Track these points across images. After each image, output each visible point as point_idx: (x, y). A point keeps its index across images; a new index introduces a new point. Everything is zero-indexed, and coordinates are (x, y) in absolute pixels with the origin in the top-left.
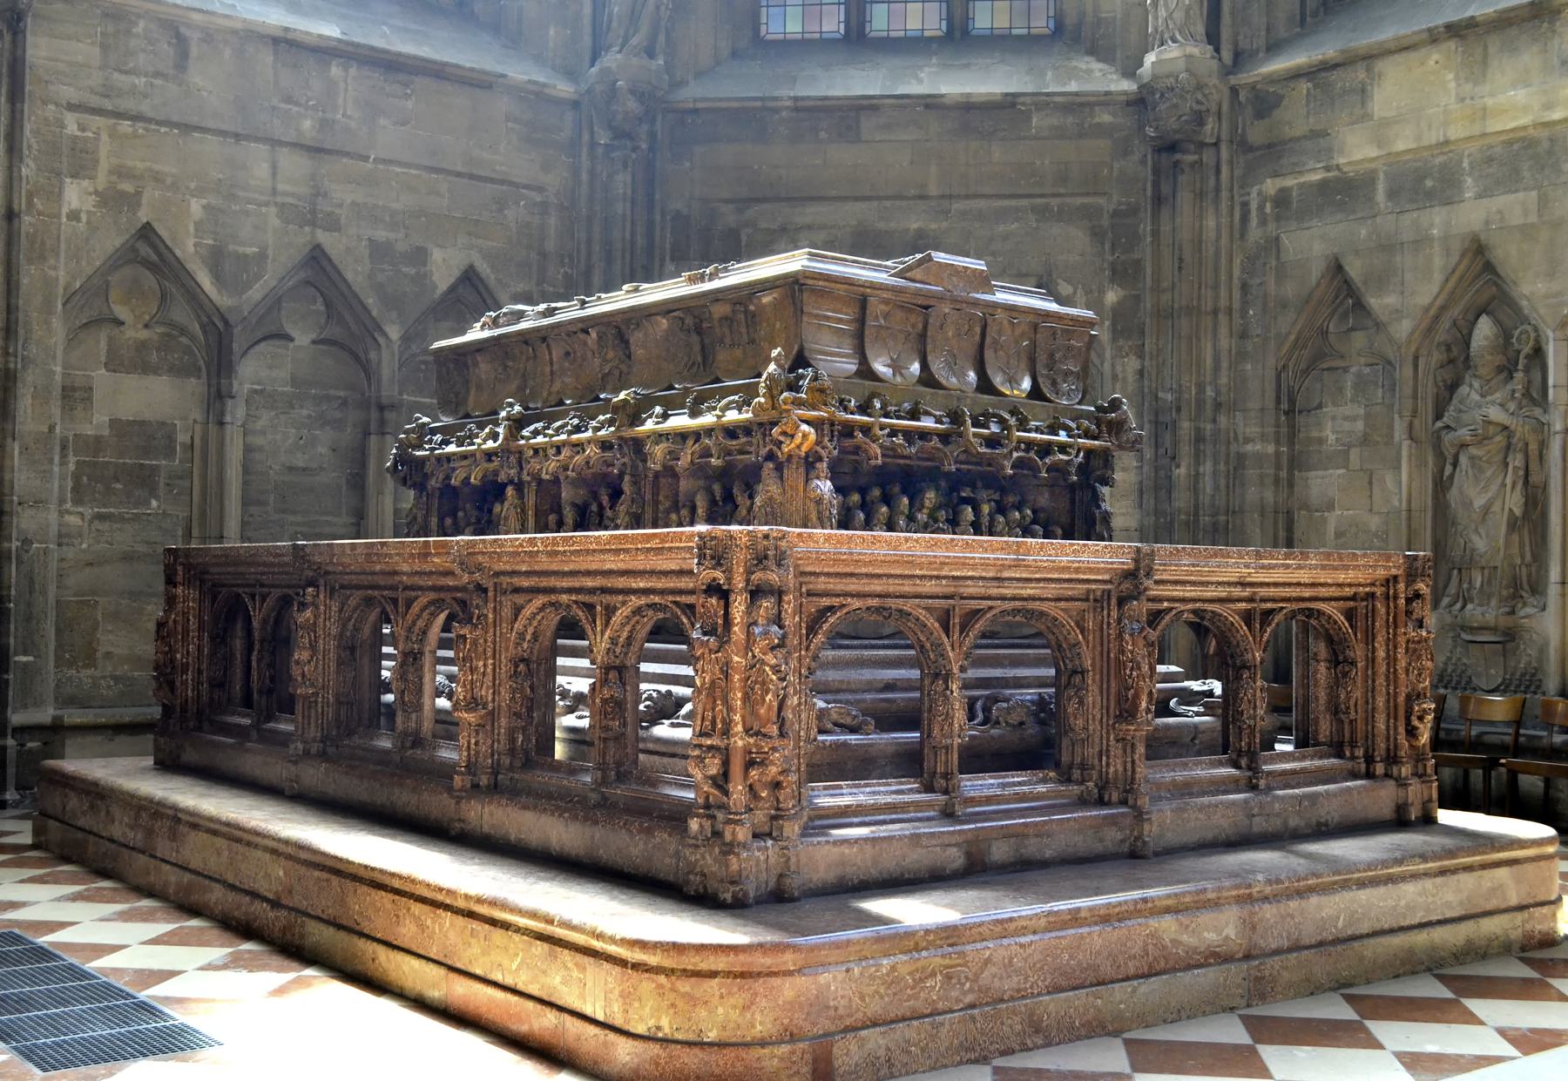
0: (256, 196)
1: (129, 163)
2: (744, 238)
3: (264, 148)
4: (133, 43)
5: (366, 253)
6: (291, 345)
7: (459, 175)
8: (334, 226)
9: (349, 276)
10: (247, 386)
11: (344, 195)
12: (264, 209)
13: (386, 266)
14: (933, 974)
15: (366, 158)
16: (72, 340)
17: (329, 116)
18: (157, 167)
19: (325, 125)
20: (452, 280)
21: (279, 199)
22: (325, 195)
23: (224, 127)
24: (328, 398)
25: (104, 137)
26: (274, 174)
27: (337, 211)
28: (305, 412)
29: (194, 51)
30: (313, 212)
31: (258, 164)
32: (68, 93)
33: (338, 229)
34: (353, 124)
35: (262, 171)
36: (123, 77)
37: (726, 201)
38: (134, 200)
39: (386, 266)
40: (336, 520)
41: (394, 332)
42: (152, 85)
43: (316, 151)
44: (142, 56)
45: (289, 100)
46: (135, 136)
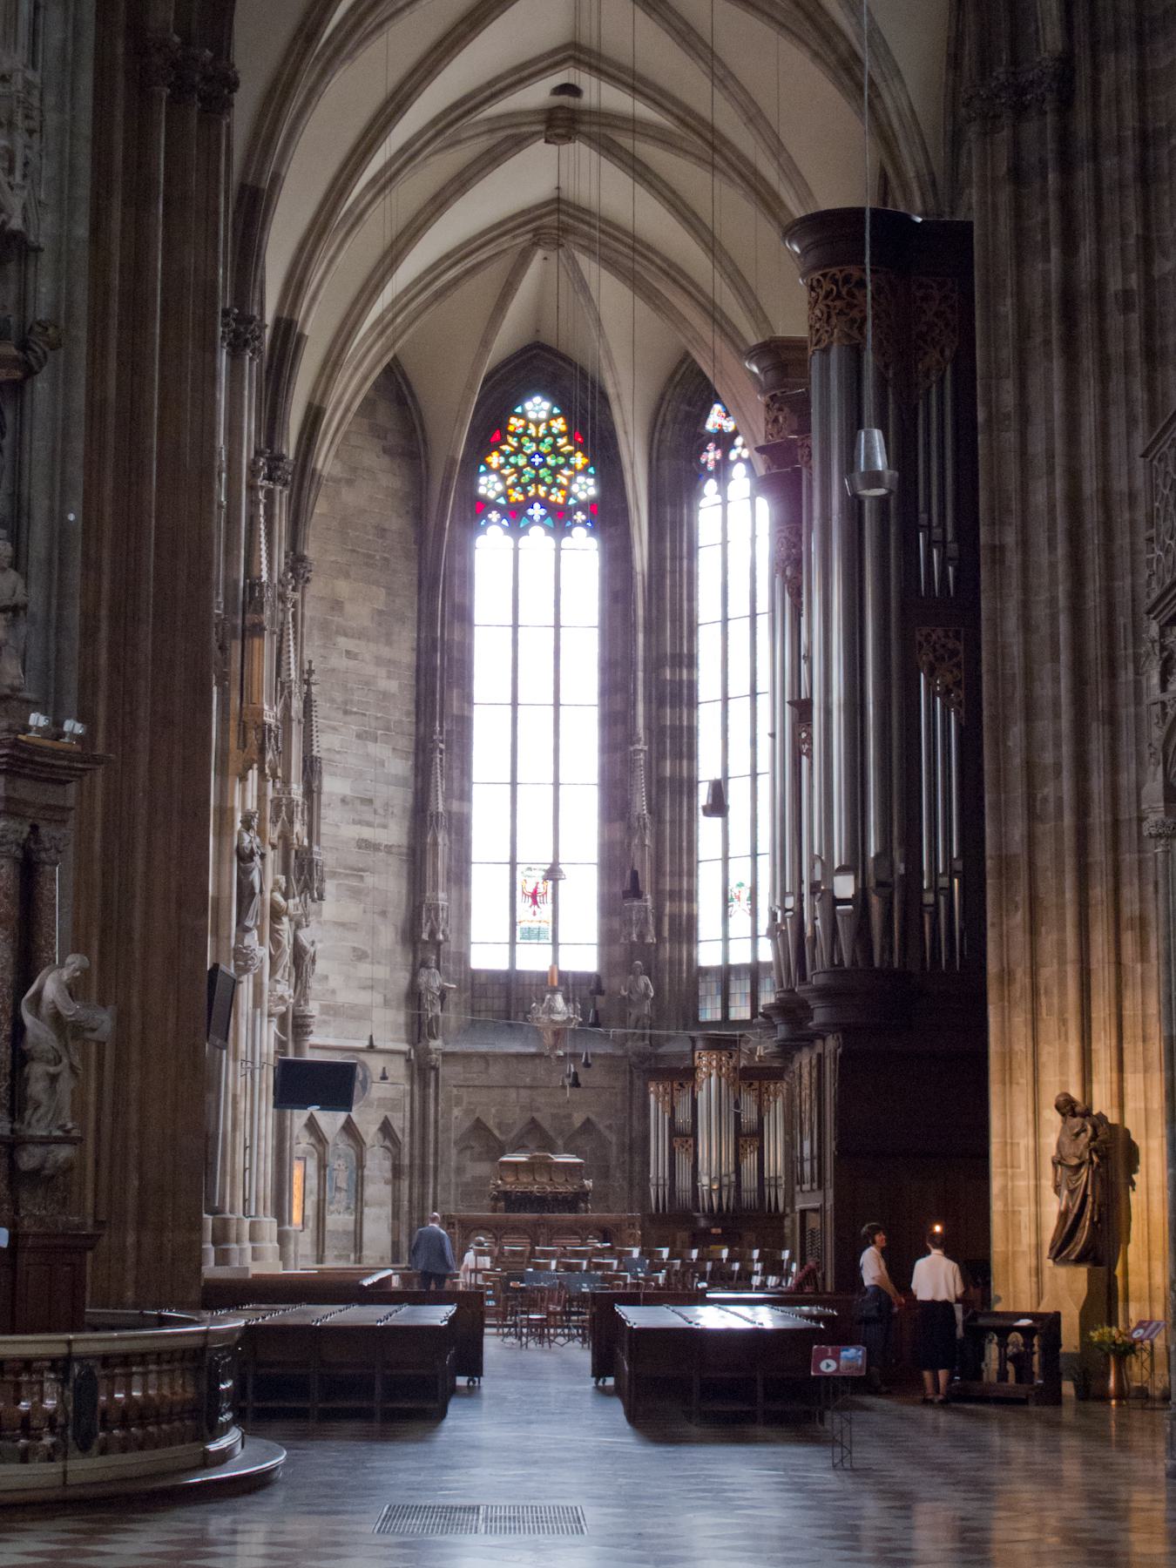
8: (538, 1110)
16: (461, 1152)
19: (534, 1079)
31: (513, 1094)
38: (473, 1111)
43: (531, 1087)
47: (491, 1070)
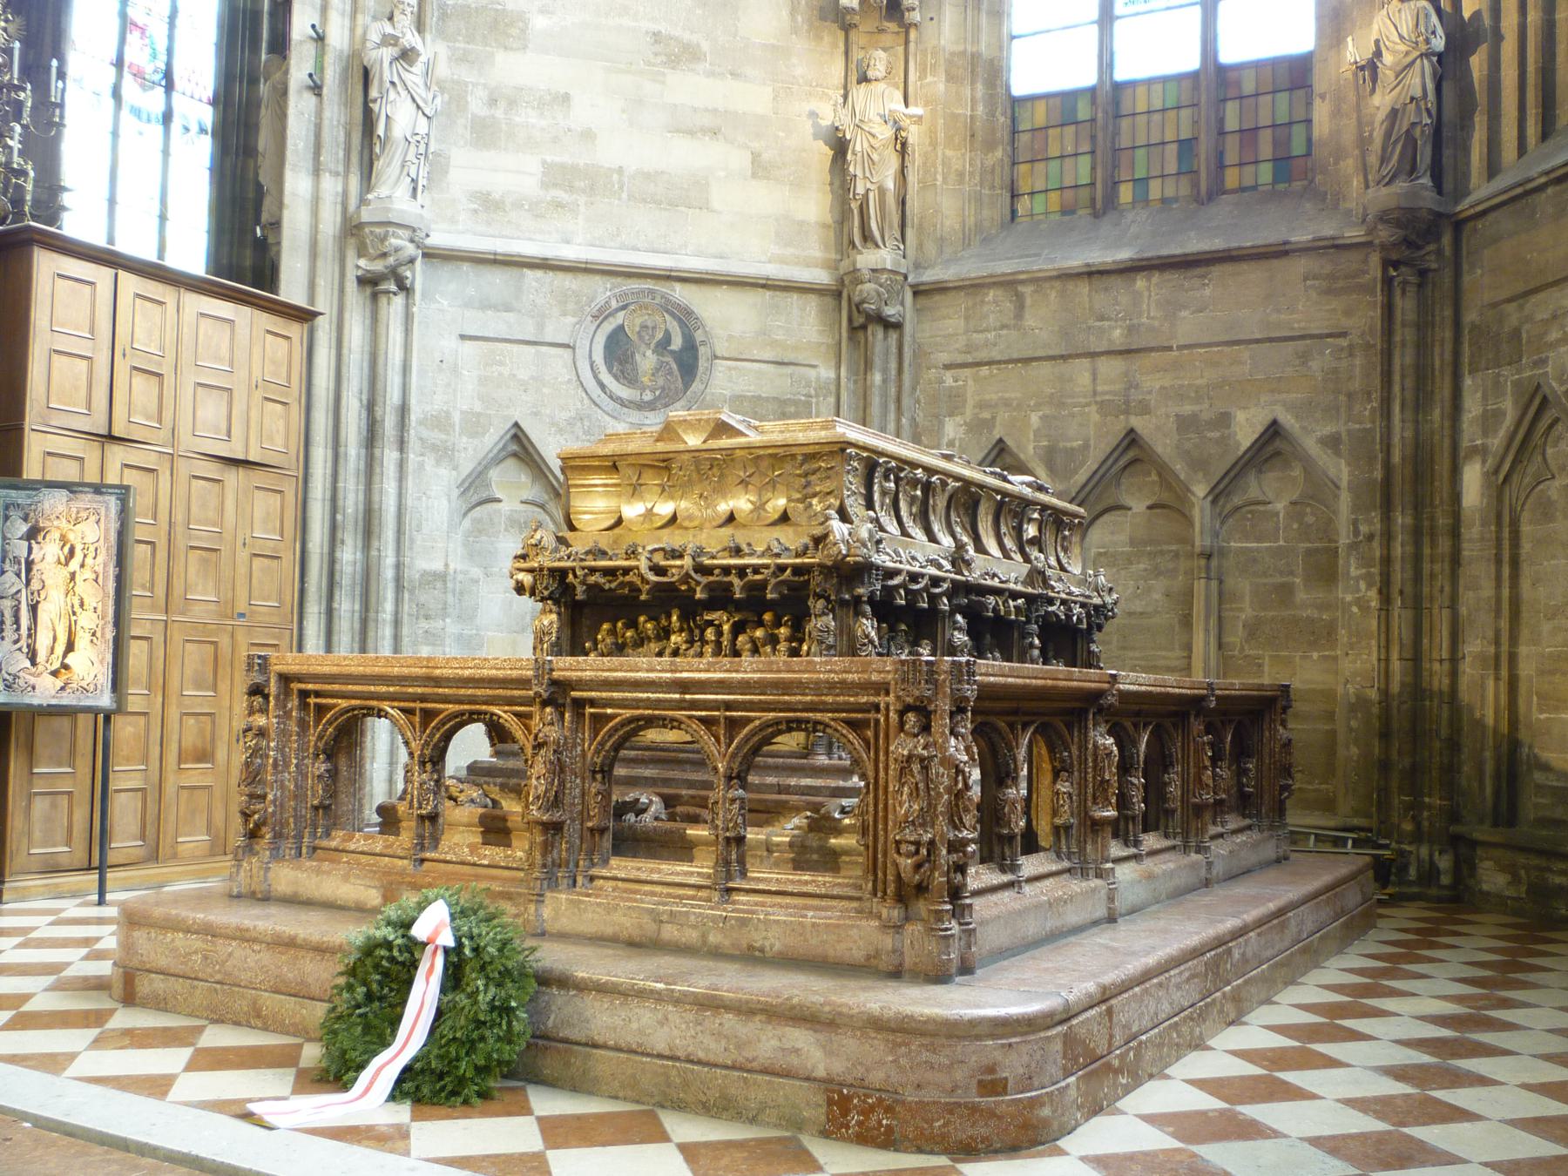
1: (987, 397)
2: (1524, 336)
3: (1086, 362)
4: (986, 308)
7: (1257, 341)
8: (1145, 409)
9: (1159, 450)
10: (1094, 551)
11: (1152, 382)
14: (196, 952)
15: (1170, 348)
18: (1007, 395)
19: (1131, 330)
20: (1256, 436)
21: (1098, 399)
22: (1137, 387)
23: (1051, 353)
24: (1162, 553)
25: (970, 382)
26: (1094, 379)
28: (1142, 566)
29: (1028, 301)
30: (1127, 403)
31: (1081, 372)
32: (945, 358)
34: (1156, 323)
35: (1084, 379)
36: (980, 336)
37: (1509, 300)
38: (989, 424)
40: (1170, 654)
41: (1200, 490)
44: (992, 317)
45: (1102, 318)
46: (992, 376)
47: (1030, 321)
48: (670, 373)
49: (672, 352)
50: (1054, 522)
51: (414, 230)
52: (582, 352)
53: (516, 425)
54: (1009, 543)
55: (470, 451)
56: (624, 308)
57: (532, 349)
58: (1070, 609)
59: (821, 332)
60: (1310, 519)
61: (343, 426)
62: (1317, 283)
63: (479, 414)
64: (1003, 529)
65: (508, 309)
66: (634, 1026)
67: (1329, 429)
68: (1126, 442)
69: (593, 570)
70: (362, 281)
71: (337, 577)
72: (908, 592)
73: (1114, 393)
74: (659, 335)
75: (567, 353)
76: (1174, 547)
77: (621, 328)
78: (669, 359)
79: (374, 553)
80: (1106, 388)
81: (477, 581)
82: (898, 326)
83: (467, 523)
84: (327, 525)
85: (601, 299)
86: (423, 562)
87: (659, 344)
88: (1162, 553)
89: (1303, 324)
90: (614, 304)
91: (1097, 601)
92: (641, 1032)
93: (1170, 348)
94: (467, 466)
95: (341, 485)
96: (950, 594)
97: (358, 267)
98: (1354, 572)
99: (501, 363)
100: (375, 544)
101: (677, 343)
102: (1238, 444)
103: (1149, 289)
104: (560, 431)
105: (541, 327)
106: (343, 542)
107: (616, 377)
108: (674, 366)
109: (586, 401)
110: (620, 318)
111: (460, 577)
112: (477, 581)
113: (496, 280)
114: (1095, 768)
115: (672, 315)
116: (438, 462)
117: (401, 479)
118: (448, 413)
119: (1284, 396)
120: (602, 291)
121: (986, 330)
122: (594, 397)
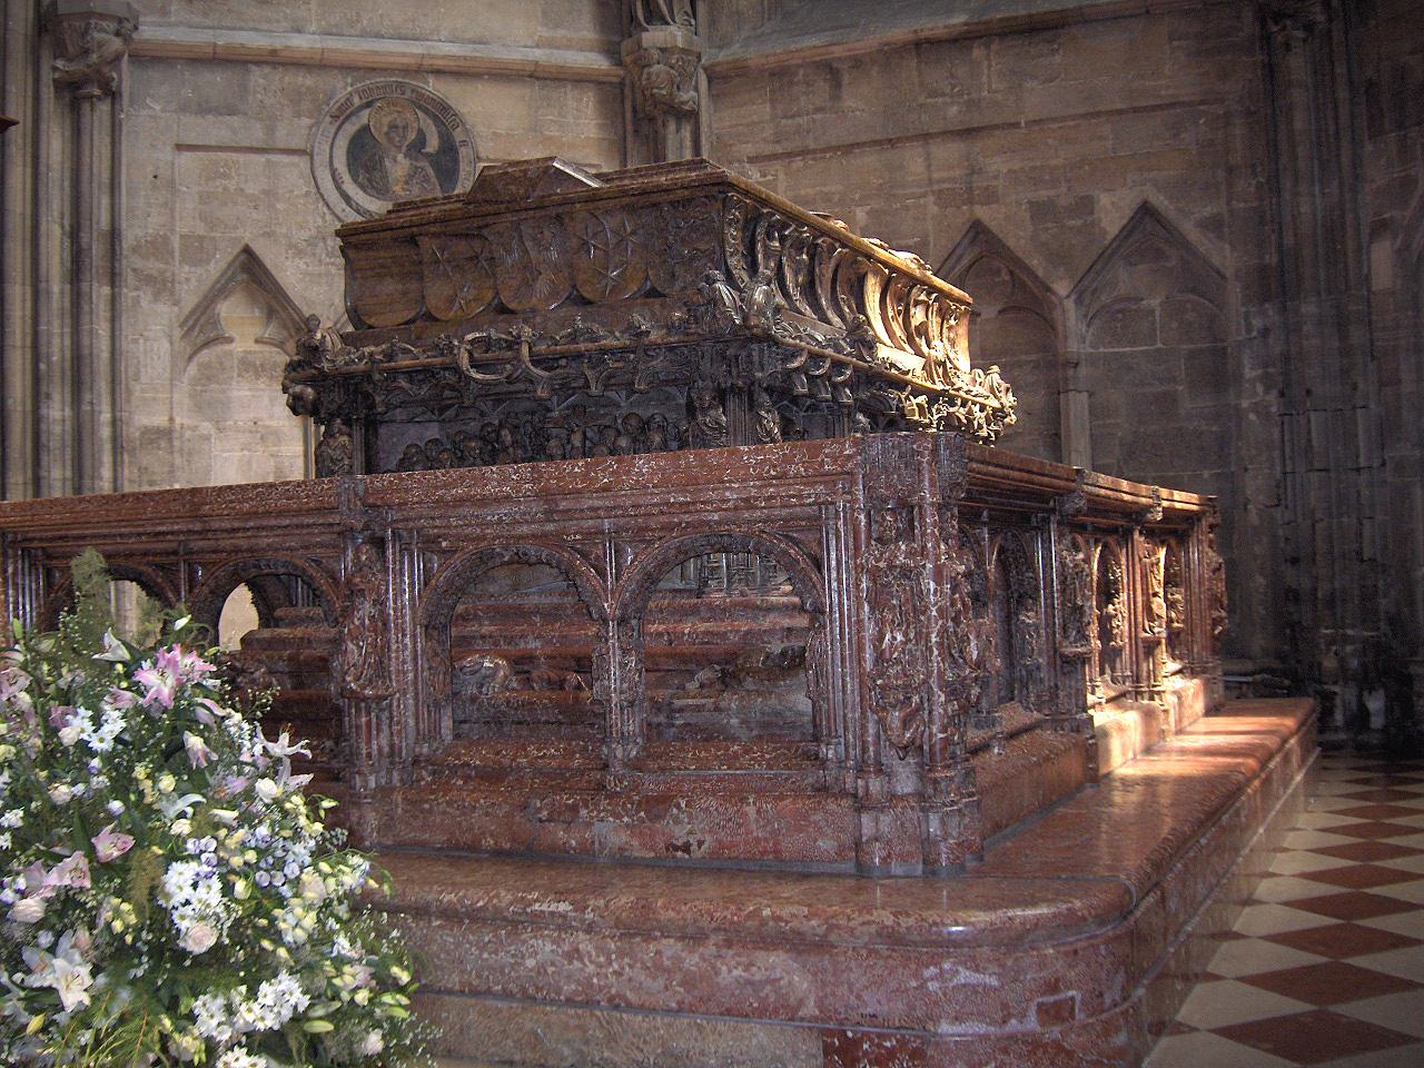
0: (915, 190)
1: (803, 192)
4: (796, 89)
5: (1027, 216)
6: (979, 320)
7: (1120, 112)
8: (991, 197)
9: (1011, 243)
12: (922, 201)
13: (1049, 225)
15: (1016, 125)
17: (974, 96)
19: (972, 104)
20: (1125, 221)
21: (936, 187)
23: (878, 137)
25: (781, 176)
27: (994, 183)
29: (846, 79)
31: (914, 161)
32: (749, 149)
33: (997, 202)
34: (999, 97)
39: (1049, 225)
42: (814, 121)
43: (968, 133)
47: (849, 102)
48: (426, 179)
49: (428, 155)
50: (940, 310)
51: (120, 21)
52: (321, 159)
53: (247, 250)
54: (899, 332)
55: (194, 283)
56: (369, 105)
57: (261, 158)
58: (970, 412)
59: (600, 127)
60: (1190, 316)
61: (43, 258)
62: (1183, 43)
63: (201, 239)
64: (890, 314)
65: (232, 112)
66: (531, 963)
67: (1209, 211)
68: (971, 235)
69: (394, 373)
70: (59, 86)
71: (44, 439)
72: (811, 379)
73: (954, 180)
74: (412, 136)
75: (303, 162)
76: (1033, 357)
77: (366, 129)
78: (425, 164)
79: (86, 408)
80: (945, 174)
81: (207, 438)
82: (693, 116)
83: (192, 369)
84: (29, 377)
85: (341, 95)
86: (145, 417)
87: (410, 147)
88: (1020, 365)
89: (1170, 92)
90: (356, 101)
91: (993, 403)
92: (541, 969)
93: (1016, 125)
94: (190, 301)
95: (43, 328)
96: (852, 385)
97: (55, 69)
98: (1248, 373)
99: (226, 176)
100: (87, 397)
101: (433, 144)
102: (1105, 232)
103: (988, 59)
104: (300, 253)
105: (271, 131)
106: (48, 396)
107: (362, 187)
108: (431, 172)
109: (329, 217)
110: (364, 117)
111: (188, 434)
112: (207, 438)
113: (216, 82)
114: (1063, 591)
115: (426, 111)
116: (156, 297)
117: (114, 319)
118: (166, 239)
119: (1153, 174)
120: (343, 88)
121: (798, 114)
122: (338, 211)
